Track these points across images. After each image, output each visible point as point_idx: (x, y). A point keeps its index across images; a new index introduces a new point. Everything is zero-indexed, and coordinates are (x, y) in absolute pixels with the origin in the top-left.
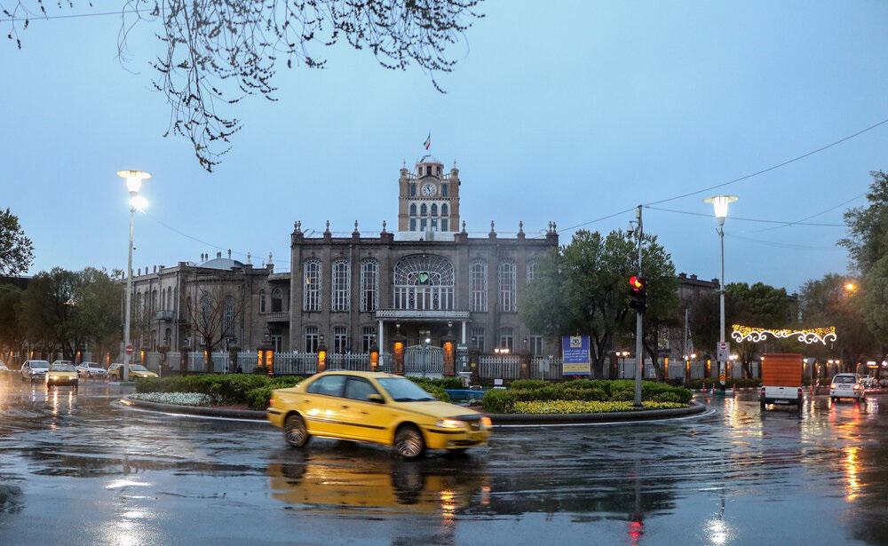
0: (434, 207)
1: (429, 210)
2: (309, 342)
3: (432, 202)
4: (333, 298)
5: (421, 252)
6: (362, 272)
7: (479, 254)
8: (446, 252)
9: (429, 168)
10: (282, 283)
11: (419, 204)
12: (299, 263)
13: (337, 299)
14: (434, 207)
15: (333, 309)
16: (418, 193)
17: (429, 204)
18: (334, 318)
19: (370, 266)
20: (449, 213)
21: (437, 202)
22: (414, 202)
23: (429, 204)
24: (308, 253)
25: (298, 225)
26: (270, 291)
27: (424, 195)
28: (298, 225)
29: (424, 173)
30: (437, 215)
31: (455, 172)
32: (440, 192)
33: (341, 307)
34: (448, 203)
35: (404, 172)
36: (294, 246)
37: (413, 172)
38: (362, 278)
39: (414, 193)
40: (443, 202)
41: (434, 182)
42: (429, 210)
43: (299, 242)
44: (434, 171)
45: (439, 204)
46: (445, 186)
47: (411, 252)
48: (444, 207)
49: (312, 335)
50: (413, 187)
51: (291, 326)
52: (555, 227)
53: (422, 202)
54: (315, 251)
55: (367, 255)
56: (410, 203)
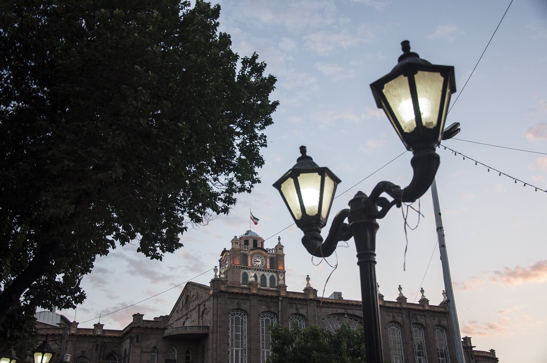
0: (263, 277)
5: (343, 311)
14: (263, 277)
21: (266, 274)
23: (259, 274)
30: (266, 286)
31: (280, 247)
32: (268, 265)
34: (275, 275)
40: (270, 274)
44: (259, 246)
45: (268, 275)
46: (272, 259)
47: (335, 311)
48: (272, 278)
54: (241, 302)
55: (294, 311)
56: (243, 271)
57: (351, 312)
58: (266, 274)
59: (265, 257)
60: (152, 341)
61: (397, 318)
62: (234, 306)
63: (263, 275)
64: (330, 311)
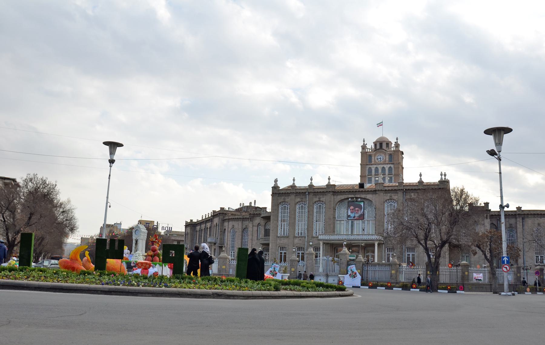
1: (380, 171)
2: (281, 256)
3: (382, 166)
4: (297, 228)
5: (353, 196)
6: (315, 210)
7: (391, 196)
8: (369, 196)
9: (381, 144)
10: (267, 218)
11: (373, 168)
12: (275, 205)
13: (299, 229)
15: (296, 235)
16: (373, 160)
17: (380, 167)
18: (296, 241)
19: (320, 206)
20: (393, 173)
21: (385, 166)
22: (371, 166)
23: (380, 167)
24: (281, 199)
25: (276, 181)
26: (263, 224)
27: (377, 161)
28: (276, 181)
29: (378, 147)
31: (397, 145)
32: (387, 160)
33: (301, 233)
34: (392, 166)
35: (364, 147)
36: (273, 195)
37: (370, 145)
38: (315, 214)
39: (370, 161)
40: (389, 166)
41: (383, 153)
42: (380, 171)
43: (277, 192)
45: (387, 167)
46: (390, 155)
49: (283, 252)
50: (370, 156)
51: (270, 245)
52: (445, 175)
53: (375, 166)
54: (286, 197)
55: (317, 199)
57: (358, 196)
58: (385, 166)
59: (385, 154)
60: (258, 220)
61: (393, 197)
62: (282, 200)
63: (383, 167)
64: (343, 197)
